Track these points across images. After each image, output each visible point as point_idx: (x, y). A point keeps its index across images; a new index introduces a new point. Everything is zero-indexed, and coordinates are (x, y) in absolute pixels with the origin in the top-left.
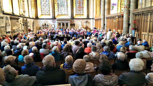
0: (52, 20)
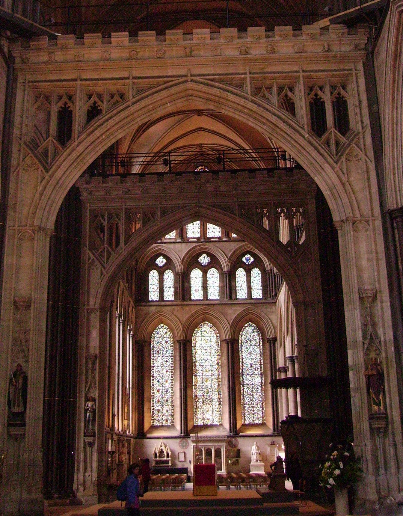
0: (178, 440)
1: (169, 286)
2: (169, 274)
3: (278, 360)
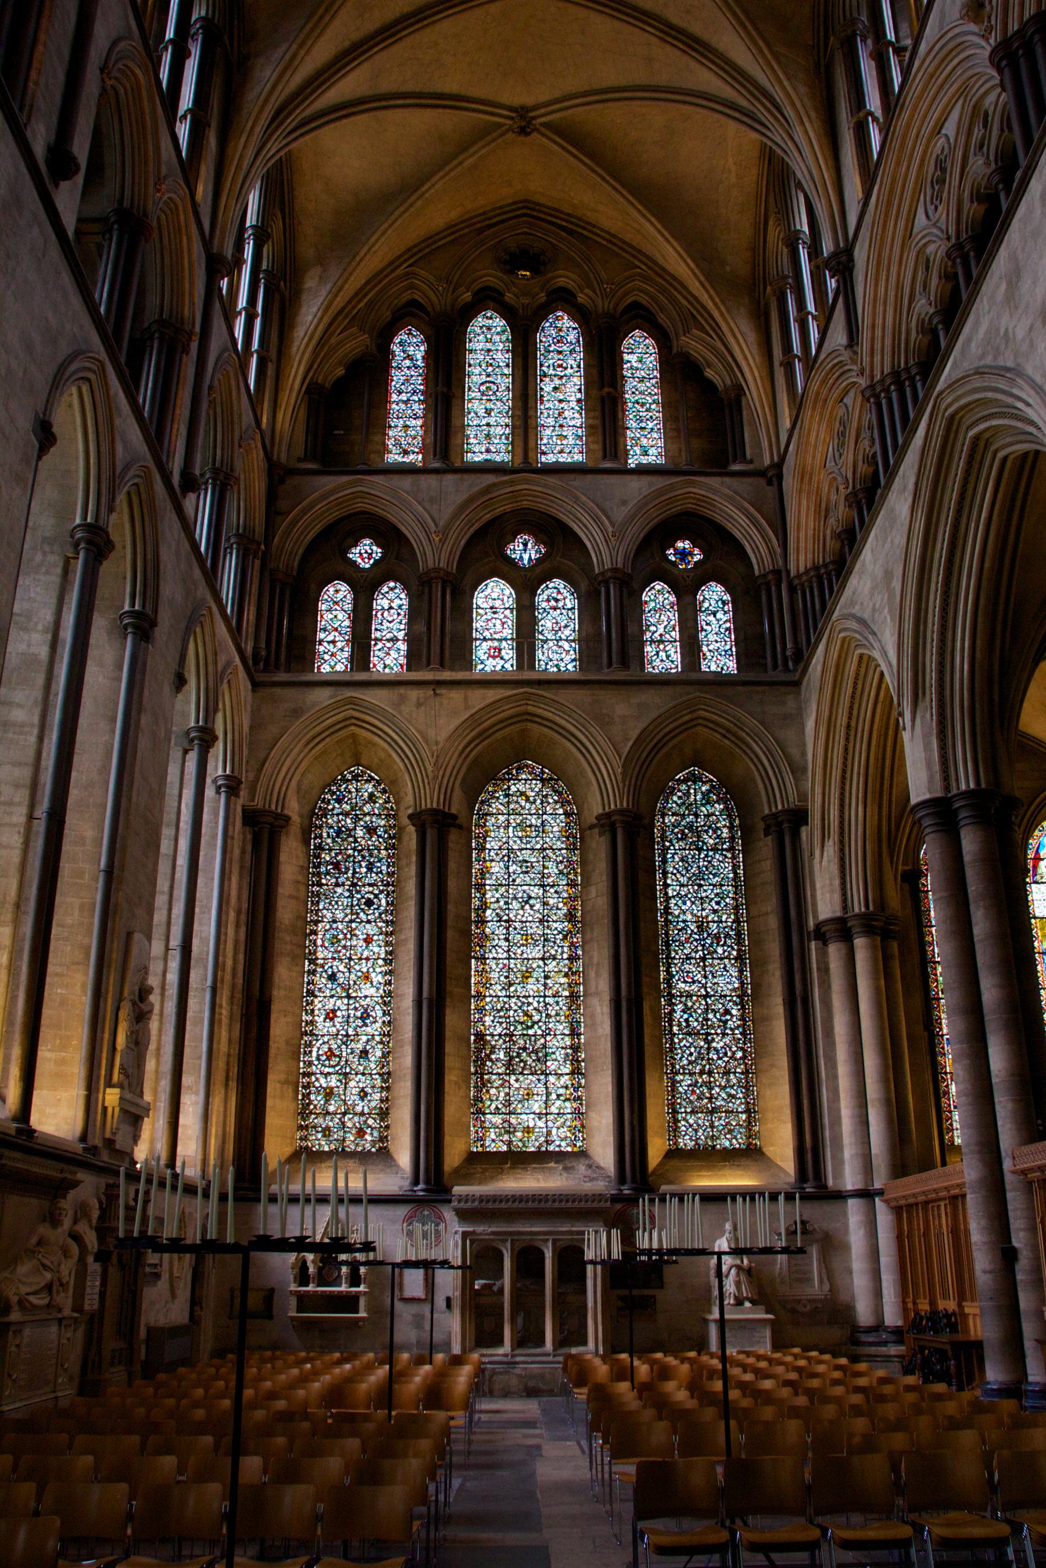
0: (402, 1211)
1: (389, 636)
2: (391, 595)
3: (814, 896)
